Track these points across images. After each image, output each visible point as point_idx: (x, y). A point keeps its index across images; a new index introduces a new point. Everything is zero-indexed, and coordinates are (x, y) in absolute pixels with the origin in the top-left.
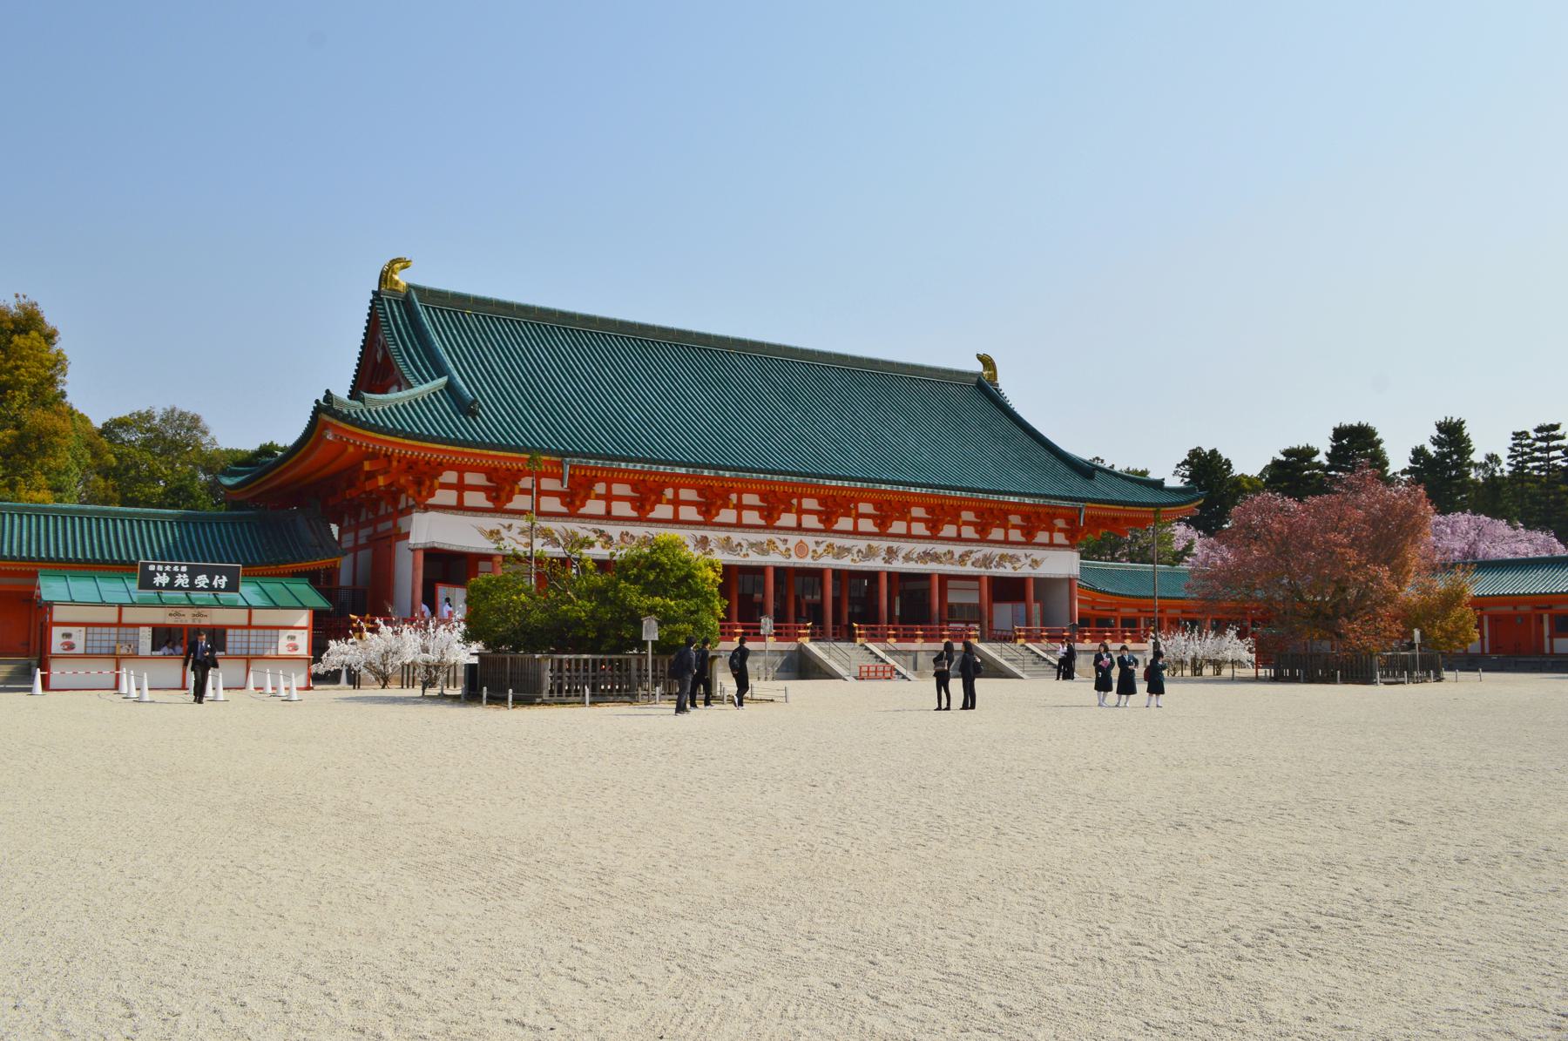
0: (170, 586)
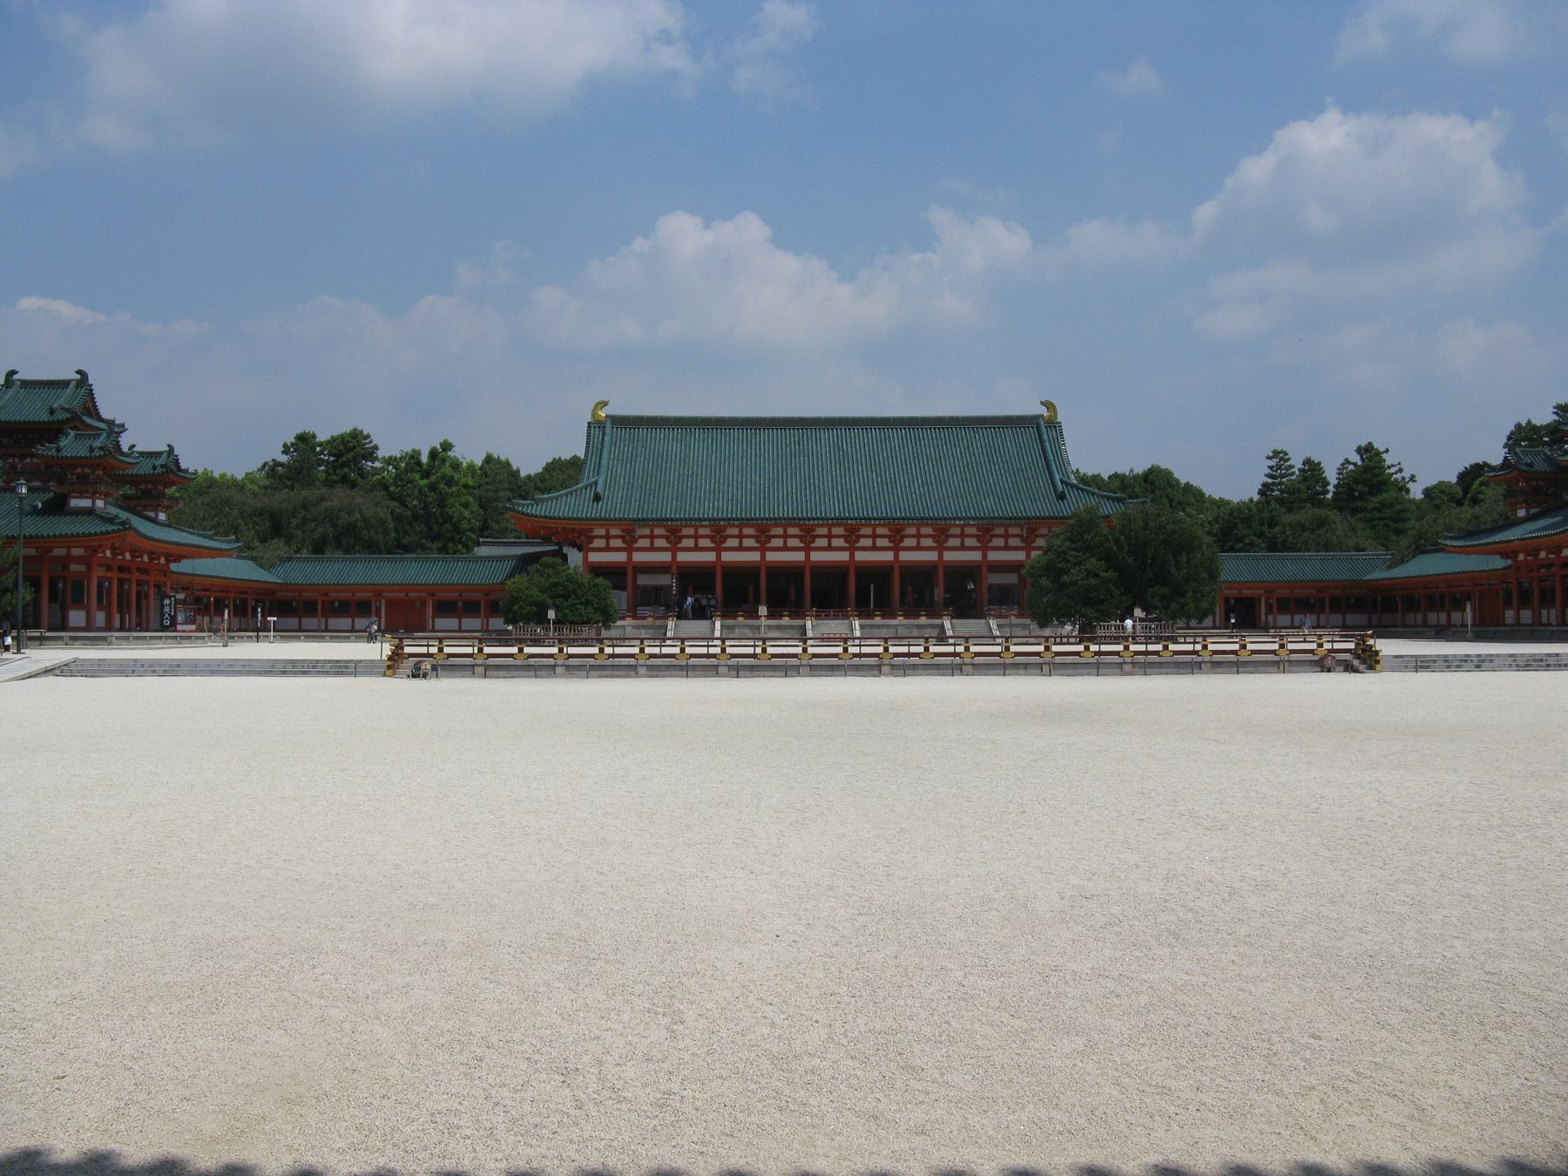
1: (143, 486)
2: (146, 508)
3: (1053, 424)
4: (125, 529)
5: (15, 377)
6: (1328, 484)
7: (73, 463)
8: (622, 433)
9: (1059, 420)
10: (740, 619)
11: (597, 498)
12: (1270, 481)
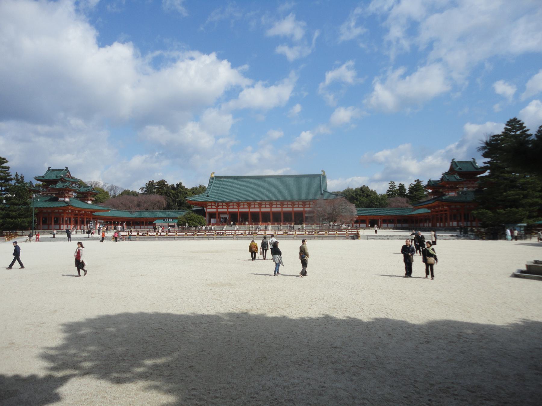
0: (166, 221)
1: (84, 195)
2: (85, 200)
3: (324, 177)
4: (69, 205)
5: (50, 168)
6: (406, 190)
7: (59, 190)
8: (218, 180)
9: (326, 175)
10: (242, 225)
11: (208, 196)
12: (389, 189)
